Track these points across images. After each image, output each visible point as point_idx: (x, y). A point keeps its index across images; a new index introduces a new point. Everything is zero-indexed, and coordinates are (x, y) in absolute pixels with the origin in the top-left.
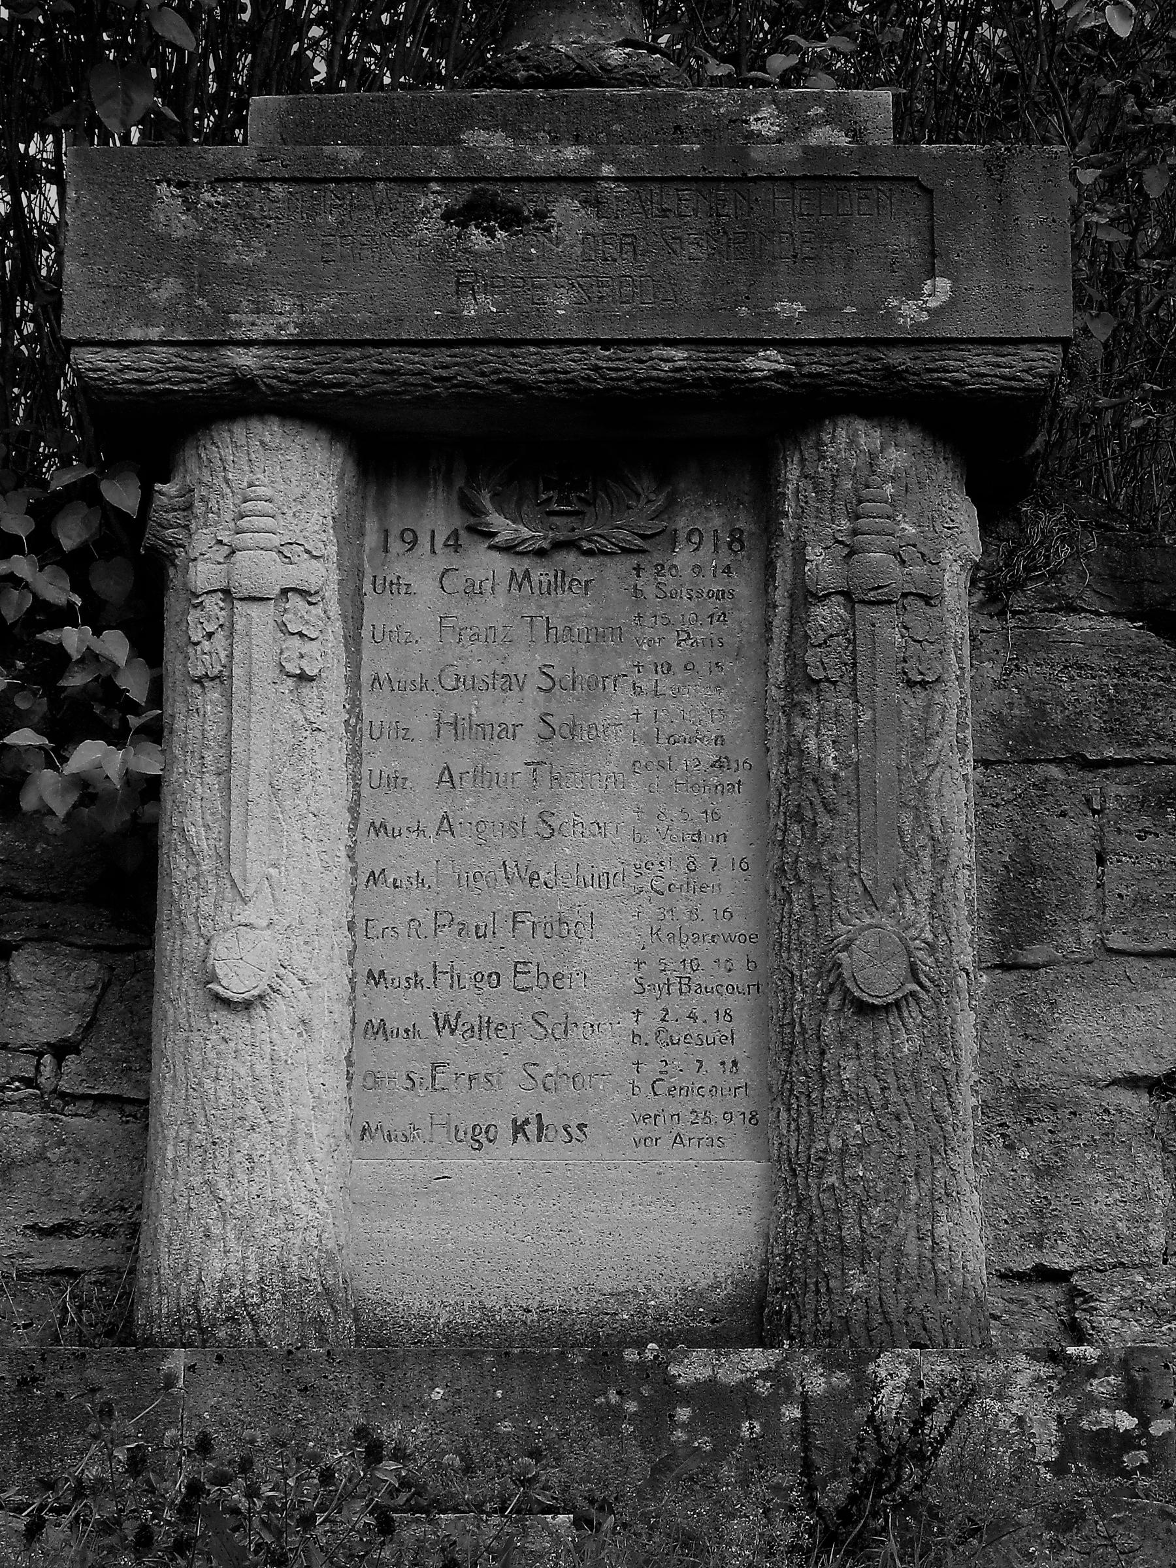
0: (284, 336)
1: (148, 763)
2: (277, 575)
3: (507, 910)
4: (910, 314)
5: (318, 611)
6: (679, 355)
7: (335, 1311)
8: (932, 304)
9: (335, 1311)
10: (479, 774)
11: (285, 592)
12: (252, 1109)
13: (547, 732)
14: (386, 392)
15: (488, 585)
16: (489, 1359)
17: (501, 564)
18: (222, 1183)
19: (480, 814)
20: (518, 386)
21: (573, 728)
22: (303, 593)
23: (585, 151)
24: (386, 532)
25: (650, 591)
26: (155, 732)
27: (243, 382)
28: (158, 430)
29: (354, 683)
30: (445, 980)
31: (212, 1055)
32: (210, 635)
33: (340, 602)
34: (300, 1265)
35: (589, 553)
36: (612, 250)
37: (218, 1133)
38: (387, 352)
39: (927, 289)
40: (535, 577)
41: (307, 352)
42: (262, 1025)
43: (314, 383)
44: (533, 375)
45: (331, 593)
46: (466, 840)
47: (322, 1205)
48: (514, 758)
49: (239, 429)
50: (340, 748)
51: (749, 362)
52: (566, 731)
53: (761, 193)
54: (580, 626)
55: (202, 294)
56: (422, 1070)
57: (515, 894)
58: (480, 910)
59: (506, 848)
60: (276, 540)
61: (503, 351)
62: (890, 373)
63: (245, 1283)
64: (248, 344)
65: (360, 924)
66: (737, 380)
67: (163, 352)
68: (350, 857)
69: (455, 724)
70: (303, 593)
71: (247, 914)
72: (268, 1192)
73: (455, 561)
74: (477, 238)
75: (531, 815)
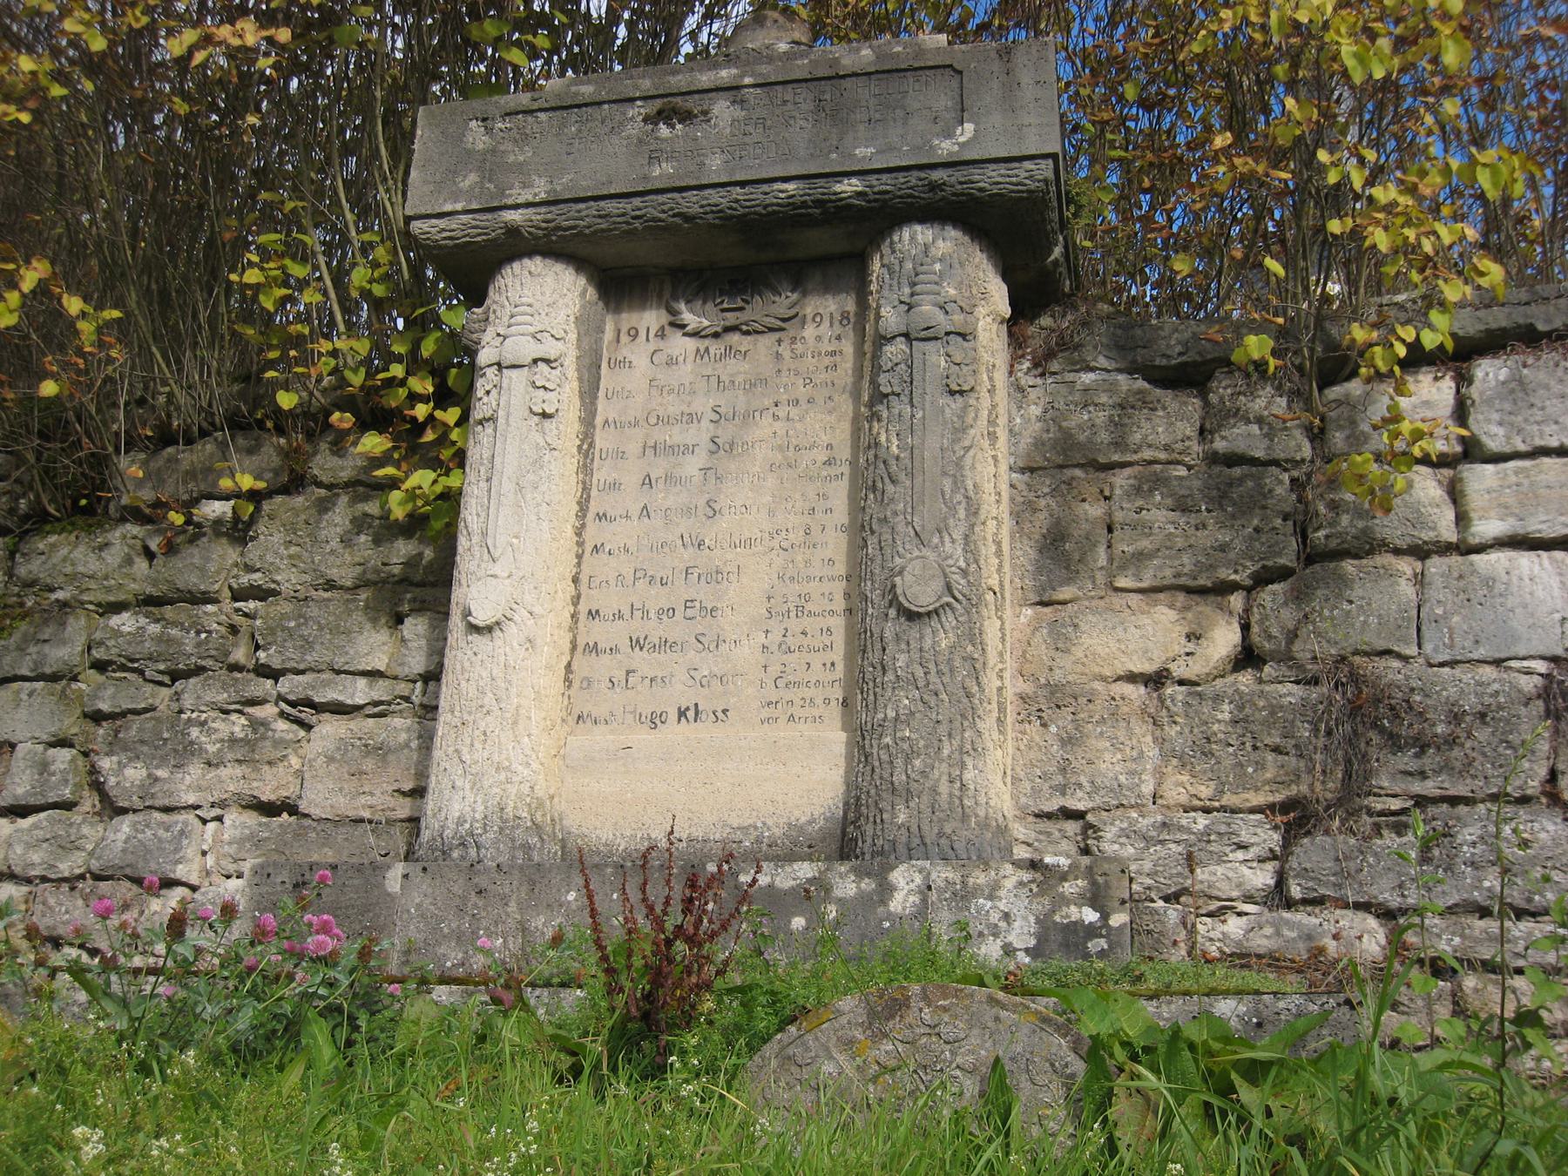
0: (537, 199)
1: (453, 481)
2: (530, 350)
3: (682, 566)
4: (946, 148)
5: (557, 372)
6: (791, 187)
7: (542, 840)
8: (961, 139)
9: (542, 840)
10: (668, 478)
11: (535, 361)
12: (489, 699)
13: (714, 448)
14: (603, 230)
15: (681, 359)
16: (609, 870)
17: (691, 344)
18: (465, 750)
19: (669, 503)
20: (687, 218)
21: (732, 445)
22: (547, 361)
23: (734, 71)
24: (619, 331)
25: (787, 354)
26: (460, 458)
27: (512, 231)
28: (472, 270)
29: (588, 421)
30: (638, 614)
31: (467, 664)
32: (488, 393)
33: (578, 370)
34: (515, 808)
35: (747, 333)
36: (750, 129)
37: (466, 716)
38: (602, 204)
39: (959, 131)
40: (712, 351)
41: (552, 208)
42: (498, 642)
43: (558, 228)
44: (696, 209)
45: (570, 363)
46: (657, 521)
47: (535, 766)
48: (692, 466)
49: (516, 265)
50: (572, 463)
51: (838, 188)
52: (727, 447)
53: (847, 83)
54: (739, 379)
55: (490, 181)
56: (619, 675)
57: (688, 555)
58: (664, 567)
59: (684, 525)
60: (532, 329)
61: (676, 195)
62: (934, 187)
63: (474, 820)
64: (516, 207)
65: (584, 578)
66: (831, 201)
67: (465, 218)
68: (579, 534)
69: (655, 448)
70: (547, 361)
71: (497, 569)
72: (496, 758)
73: (661, 344)
74: (664, 130)
75: (702, 502)
